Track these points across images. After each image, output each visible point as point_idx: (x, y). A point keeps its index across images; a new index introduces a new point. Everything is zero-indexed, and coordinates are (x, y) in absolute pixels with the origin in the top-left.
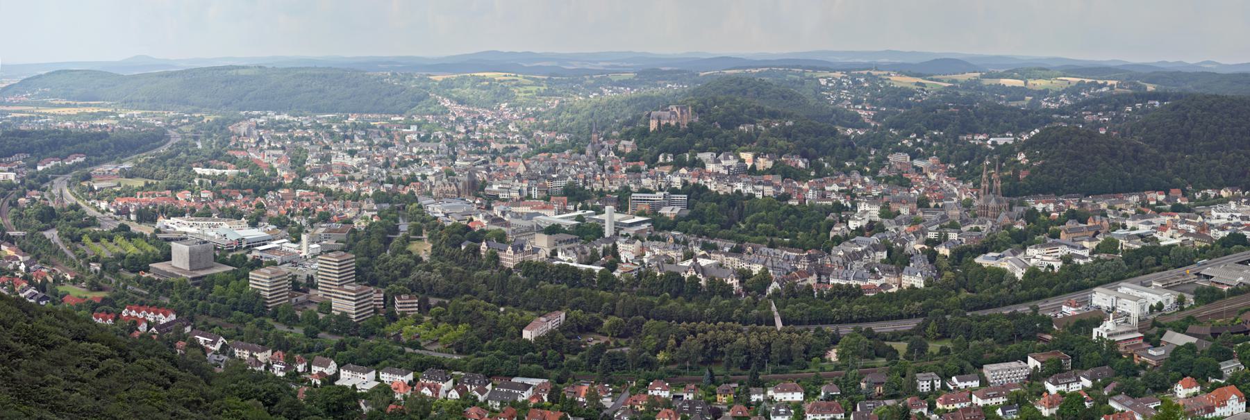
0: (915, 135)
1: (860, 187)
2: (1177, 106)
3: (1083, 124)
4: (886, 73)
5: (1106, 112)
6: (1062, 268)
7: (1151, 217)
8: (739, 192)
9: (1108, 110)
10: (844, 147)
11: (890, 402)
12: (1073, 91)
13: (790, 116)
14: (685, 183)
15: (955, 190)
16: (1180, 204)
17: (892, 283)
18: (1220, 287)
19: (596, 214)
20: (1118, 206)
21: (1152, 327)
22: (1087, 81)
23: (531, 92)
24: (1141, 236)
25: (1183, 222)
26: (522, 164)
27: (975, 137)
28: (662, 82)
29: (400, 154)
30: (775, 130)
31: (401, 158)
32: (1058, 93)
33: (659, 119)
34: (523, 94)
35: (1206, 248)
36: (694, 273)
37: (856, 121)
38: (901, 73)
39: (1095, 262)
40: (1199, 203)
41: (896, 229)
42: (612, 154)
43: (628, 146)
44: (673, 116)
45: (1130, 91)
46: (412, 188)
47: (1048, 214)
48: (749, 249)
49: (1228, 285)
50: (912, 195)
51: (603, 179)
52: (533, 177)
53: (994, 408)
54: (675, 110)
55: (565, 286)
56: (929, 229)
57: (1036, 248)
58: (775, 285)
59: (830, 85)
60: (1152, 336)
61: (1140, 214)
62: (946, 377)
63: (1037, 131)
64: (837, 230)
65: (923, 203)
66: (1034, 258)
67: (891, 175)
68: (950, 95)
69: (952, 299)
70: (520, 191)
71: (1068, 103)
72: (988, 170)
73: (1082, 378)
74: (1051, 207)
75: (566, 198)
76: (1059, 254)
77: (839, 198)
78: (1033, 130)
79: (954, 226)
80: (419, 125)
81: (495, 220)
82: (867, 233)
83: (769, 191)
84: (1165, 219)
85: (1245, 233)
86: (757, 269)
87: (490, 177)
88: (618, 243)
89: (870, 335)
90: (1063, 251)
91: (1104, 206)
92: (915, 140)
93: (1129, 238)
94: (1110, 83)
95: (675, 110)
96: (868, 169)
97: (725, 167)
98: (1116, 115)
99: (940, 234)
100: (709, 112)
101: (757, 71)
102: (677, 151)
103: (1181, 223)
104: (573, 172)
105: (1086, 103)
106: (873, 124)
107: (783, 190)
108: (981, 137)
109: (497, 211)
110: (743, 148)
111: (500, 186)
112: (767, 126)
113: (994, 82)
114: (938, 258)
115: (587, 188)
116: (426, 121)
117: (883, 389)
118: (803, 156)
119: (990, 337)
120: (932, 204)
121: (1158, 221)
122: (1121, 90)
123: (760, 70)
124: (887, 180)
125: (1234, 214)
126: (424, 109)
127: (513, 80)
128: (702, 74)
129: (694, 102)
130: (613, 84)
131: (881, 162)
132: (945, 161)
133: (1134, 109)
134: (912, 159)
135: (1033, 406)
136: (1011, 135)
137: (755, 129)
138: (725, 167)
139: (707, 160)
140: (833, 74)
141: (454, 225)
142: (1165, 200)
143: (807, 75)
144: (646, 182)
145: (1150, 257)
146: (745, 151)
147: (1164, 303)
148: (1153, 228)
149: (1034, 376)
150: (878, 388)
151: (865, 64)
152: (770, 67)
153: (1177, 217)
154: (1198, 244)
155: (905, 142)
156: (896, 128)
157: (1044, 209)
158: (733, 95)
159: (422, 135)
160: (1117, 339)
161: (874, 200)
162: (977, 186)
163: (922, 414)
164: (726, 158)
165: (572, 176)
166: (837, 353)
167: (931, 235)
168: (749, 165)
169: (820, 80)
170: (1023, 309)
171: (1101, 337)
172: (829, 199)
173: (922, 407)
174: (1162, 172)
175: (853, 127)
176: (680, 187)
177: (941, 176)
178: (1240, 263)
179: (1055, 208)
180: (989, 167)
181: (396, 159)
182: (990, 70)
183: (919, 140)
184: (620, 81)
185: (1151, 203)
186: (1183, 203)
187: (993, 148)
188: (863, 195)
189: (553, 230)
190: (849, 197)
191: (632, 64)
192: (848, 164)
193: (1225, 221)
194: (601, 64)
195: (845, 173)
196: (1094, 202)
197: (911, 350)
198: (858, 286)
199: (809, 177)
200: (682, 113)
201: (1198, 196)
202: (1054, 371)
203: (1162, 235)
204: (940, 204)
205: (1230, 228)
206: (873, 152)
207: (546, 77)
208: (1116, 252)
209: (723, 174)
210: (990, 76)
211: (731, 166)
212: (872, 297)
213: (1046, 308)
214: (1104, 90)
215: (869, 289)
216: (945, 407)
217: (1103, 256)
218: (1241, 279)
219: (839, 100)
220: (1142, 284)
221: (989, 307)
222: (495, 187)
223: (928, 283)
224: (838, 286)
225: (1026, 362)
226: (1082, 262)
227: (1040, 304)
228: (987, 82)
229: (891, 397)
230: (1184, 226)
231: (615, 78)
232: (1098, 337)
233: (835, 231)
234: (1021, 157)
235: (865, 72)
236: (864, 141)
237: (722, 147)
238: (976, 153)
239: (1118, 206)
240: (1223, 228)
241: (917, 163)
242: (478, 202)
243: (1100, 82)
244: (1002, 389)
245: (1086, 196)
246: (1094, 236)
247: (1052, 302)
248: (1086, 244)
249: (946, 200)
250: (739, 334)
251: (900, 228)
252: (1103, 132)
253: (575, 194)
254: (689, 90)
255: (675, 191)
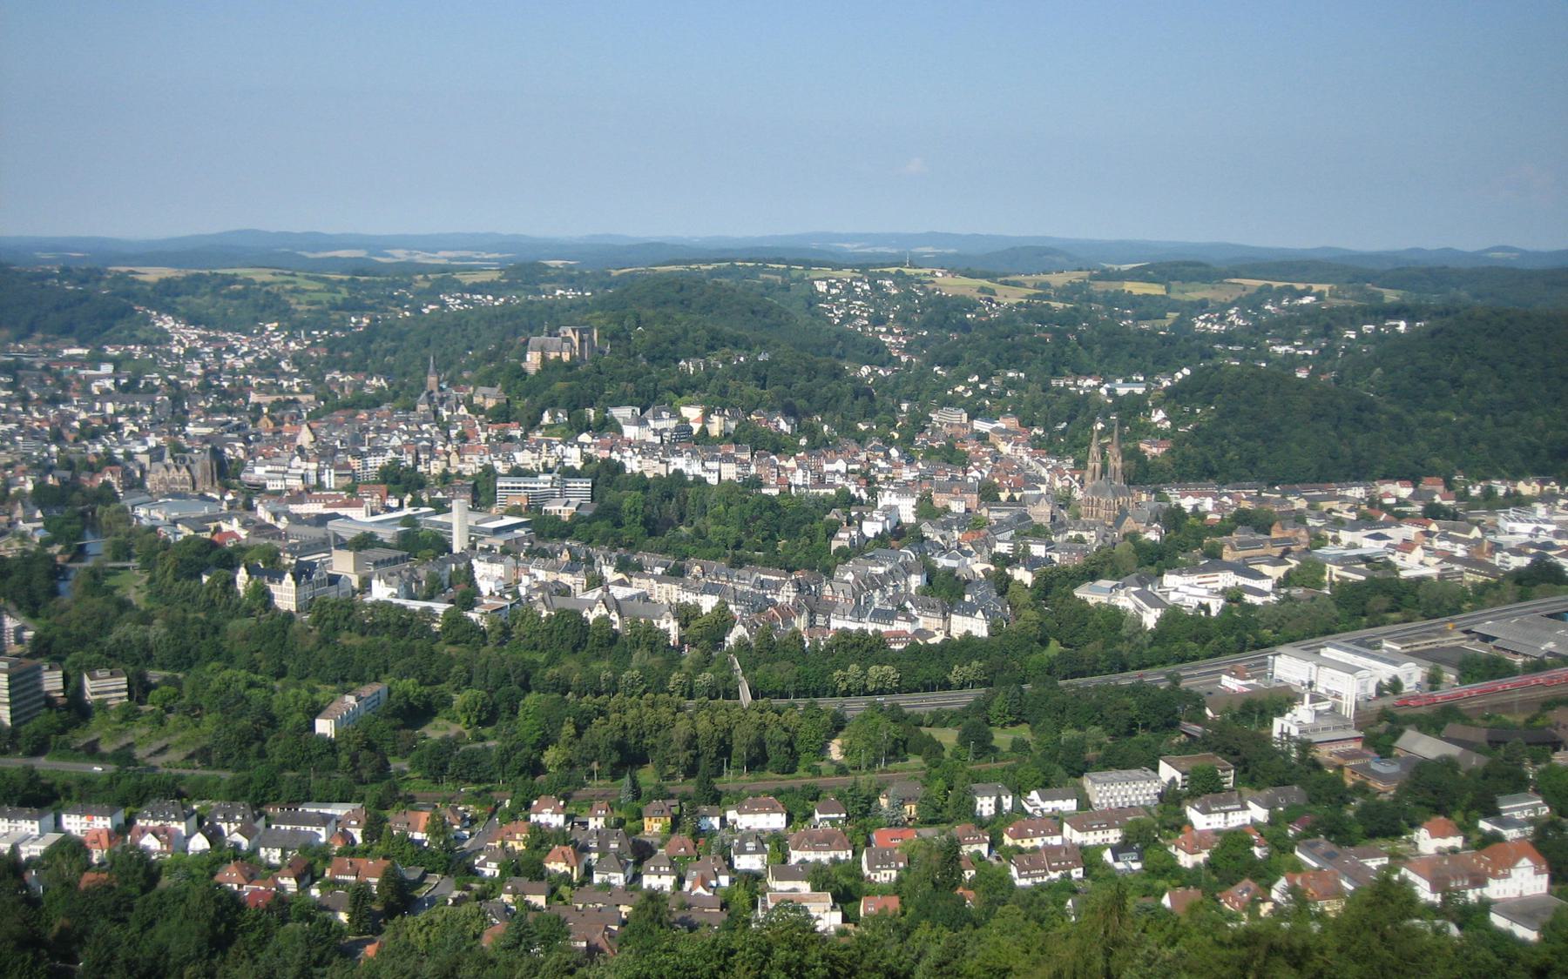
0: (976, 378)
1: (882, 464)
2: (1440, 330)
3: (1267, 360)
4: (928, 271)
5: (1308, 341)
6: (1224, 610)
7: (1387, 525)
8: (678, 473)
9: (1312, 336)
10: (856, 398)
11: (928, 832)
12: (1251, 303)
13: (764, 345)
14: (588, 460)
15: (1044, 473)
16: (1439, 505)
17: (934, 627)
18: (1509, 657)
19: (437, 513)
20: (1325, 505)
21: (1380, 721)
22: (1276, 285)
23: (320, 302)
24: (1366, 559)
25: (1444, 537)
26: (305, 428)
27: (1079, 383)
28: (548, 287)
29: (83, 416)
30: (741, 366)
31: (85, 423)
32: (1225, 307)
33: (543, 349)
34: (306, 307)
35: (1486, 585)
36: (604, 611)
37: (876, 353)
38: (953, 271)
39: (1281, 602)
40: (1474, 503)
41: (943, 538)
42: (463, 411)
43: (489, 399)
44: (566, 345)
45: (1353, 304)
46: (108, 477)
47: (1202, 516)
48: (696, 569)
49: (1525, 655)
50: (970, 480)
51: (448, 454)
52: (326, 453)
53: (1099, 848)
54: (570, 333)
55: (385, 638)
56: (999, 537)
57: (1180, 574)
58: (739, 631)
59: (834, 291)
60: (1378, 736)
61: (1366, 520)
62: (1019, 791)
63: (1186, 371)
64: (843, 538)
65: (988, 493)
66: (1176, 590)
67: (936, 445)
68: (1034, 312)
69: (1035, 657)
70: (303, 477)
71: (1241, 323)
72: (1100, 437)
73: (1250, 804)
74: (1208, 504)
75: (384, 487)
76: (1220, 586)
77: (847, 484)
78: (1180, 369)
79: (1039, 533)
80: (116, 362)
81: (261, 528)
82: (894, 543)
83: (730, 471)
84: (1410, 531)
85: (1562, 561)
86: (708, 603)
87: (248, 453)
88: (474, 562)
89: (898, 716)
90: (1228, 579)
91: (1300, 504)
92: (976, 385)
93: (1342, 561)
94: (1316, 288)
95: (570, 333)
96: (896, 436)
97: (656, 432)
98: (1328, 346)
99: (1016, 549)
100: (628, 338)
101: (710, 267)
102: (574, 405)
103: (1440, 539)
104: (396, 442)
105: (1277, 323)
106: (904, 359)
107: (753, 470)
108: (1090, 382)
109: (263, 513)
110: (685, 398)
111: (269, 468)
112: (726, 362)
113: (1113, 286)
114: (1011, 588)
115: (421, 468)
116: (130, 356)
117: (917, 808)
118: (789, 411)
119: (1095, 724)
120: (1004, 496)
121: (1397, 534)
122: (1337, 303)
123: (715, 265)
124: (930, 453)
125: (1541, 526)
126: (126, 332)
127: (288, 282)
128: (615, 273)
129: (602, 321)
130: (465, 289)
131: (919, 423)
132: (1027, 423)
133: (1361, 336)
134: (971, 417)
135: (1164, 848)
136: (1141, 379)
137: (707, 365)
138: (656, 432)
140: (838, 273)
141: (188, 540)
142: (1412, 496)
143: (795, 274)
144: (523, 458)
145: (1381, 597)
146: (688, 404)
147: (1403, 679)
148: (1389, 546)
149: (1171, 799)
150: (908, 807)
151: (892, 255)
152: (732, 260)
153: (1434, 527)
154: (1470, 577)
155: (960, 389)
156: (943, 365)
157: (1195, 507)
158: (669, 310)
159: (124, 381)
160: (1315, 738)
161: (904, 489)
162: (1080, 465)
163: (978, 852)
164: (657, 417)
165: (394, 448)
166: (842, 747)
167: (1003, 548)
168: (696, 428)
169: (817, 283)
170: (1156, 678)
171: (1288, 735)
172: (831, 485)
173: (980, 842)
174: (1407, 448)
175: (870, 364)
176: (578, 466)
177: (1020, 447)
178: (1550, 616)
179: (1215, 505)
180: (1102, 434)
181: (76, 424)
182: (1107, 266)
183: (983, 386)
184: (475, 283)
185: (1387, 501)
186: (1445, 503)
187: (1110, 401)
188: (887, 478)
189: (363, 543)
190: (863, 482)
191: (496, 255)
192: (862, 427)
193: (1525, 538)
194: (441, 254)
195: (858, 442)
196: (1283, 497)
197: (964, 741)
198: (877, 633)
199: (797, 448)
200: (581, 341)
201: (1475, 491)
202: (1205, 789)
203: (1403, 559)
204: (1017, 496)
205: (1532, 551)
206: (904, 407)
207: (346, 277)
208: (1321, 585)
210: (1107, 276)
211: (665, 430)
212: (900, 651)
213: (1193, 678)
214: (1307, 300)
215: (898, 636)
216: (1019, 842)
217: (1296, 592)
218: (1551, 645)
219: (848, 317)
220: (1361, 643)
221: (1095, 672)
222: (260, 471)
223: (994, 629)
224: (845, 633)
225: (1156, 770)
226: (1258, 601)
227: (1184, 670)
228: (1100, 287)
229: (931, 823)
230: (1445, 545)
231: (468, 279)
232: (1282, 733)
233: (840, 539)
234: (1158, 416)
235: (893, 270)
236: (893, 389)
237: (647, 400)
238: (1082, 409)
239: (1325, 505)
240: (1517, 552)
241: (980, 425)
242: (229, 497)
243: (1300, 286)
244: (1109, 818)
245: (1271, 485)
246: (1282, 557)
247: (1205, 666)
248: (1266, 569)
249: (1027, 489)
250: (679, 715)
251: (949, 536)
252: (1302, 374)
253: (399, 480)
254: (593, 301)
255: (570, 473)
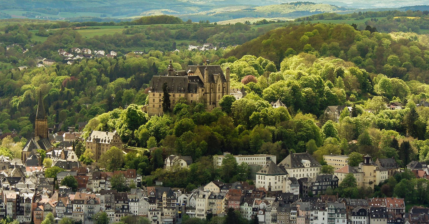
139: (259, 167)
164: (297, 164)
209: (289, 194)
211: (305, 179)
